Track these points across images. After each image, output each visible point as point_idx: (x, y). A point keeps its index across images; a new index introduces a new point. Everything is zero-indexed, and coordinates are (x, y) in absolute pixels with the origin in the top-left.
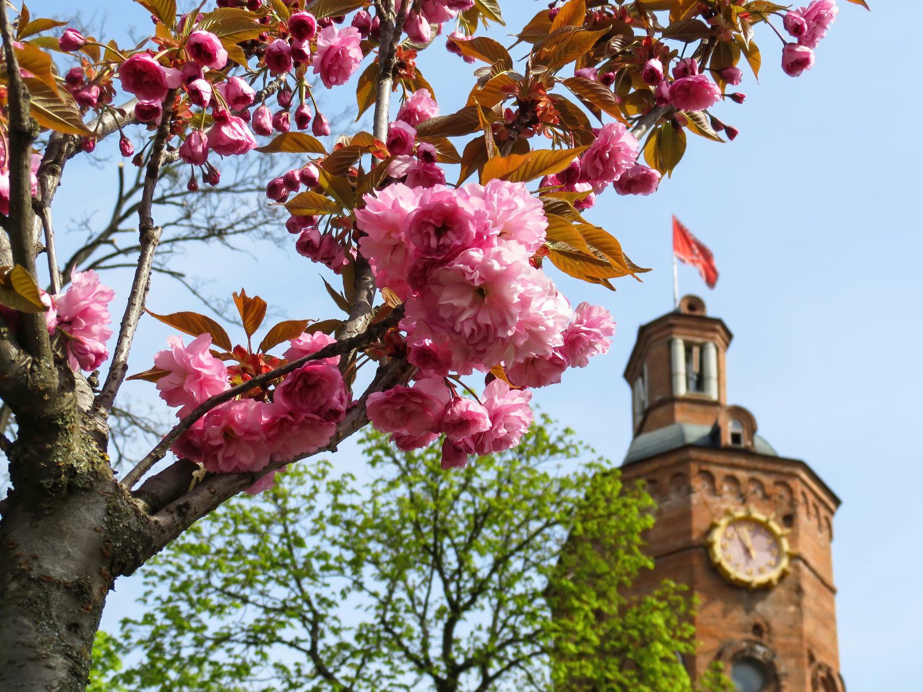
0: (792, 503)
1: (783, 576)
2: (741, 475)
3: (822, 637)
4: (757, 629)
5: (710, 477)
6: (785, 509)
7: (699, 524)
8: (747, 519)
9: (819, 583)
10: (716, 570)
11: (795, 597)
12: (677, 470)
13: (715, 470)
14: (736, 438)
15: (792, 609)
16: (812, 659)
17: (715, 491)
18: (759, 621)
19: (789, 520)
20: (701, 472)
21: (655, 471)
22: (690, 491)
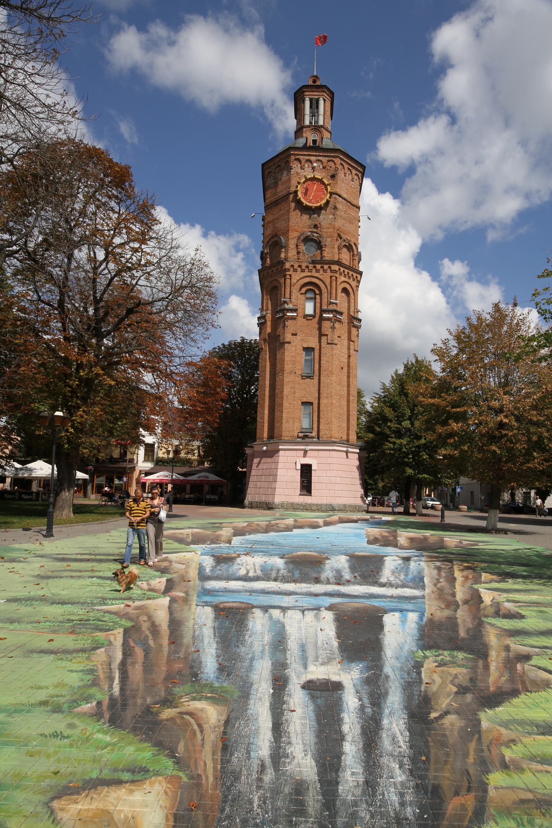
0: (336, 169)
1: (328, 202)
2: (313, 158)
3: (348, 227)
4: (316, 226)
5: (299, 160)
6: (332, 172)
7: (294, 182)
8: (313, 179)
9: (349, 204)
10: (299, 203)
11: (333, 211)
13: (301, 157)
14: (314, 141)
15: (331, 216)
16: (341, 238)
17: (302, 168)
18: (317, 223)
19: (333, 177)
20: (296, 159)
21: (279, 161)
22: (291, 168)
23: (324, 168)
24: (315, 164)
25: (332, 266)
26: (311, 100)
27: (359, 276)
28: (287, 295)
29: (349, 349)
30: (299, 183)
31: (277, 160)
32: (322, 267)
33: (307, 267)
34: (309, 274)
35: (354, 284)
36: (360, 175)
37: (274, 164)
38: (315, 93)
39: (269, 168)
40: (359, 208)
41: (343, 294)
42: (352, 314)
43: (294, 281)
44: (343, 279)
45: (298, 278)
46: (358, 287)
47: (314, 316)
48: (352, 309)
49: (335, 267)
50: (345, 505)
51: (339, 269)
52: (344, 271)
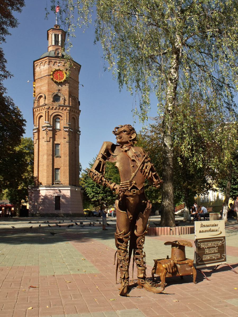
1: (65, 80)
12: (46, 61)
16: (71, 95)
18: (60, 89)
23: (63, 65)
24: (59, 65)
25: (67, 108)
26: (55, 35)
27: (79, 112)
28: (47, 120)
29: (75, 144)
30: (52, 71)
31: (41, 60)
32: (63, 108)
33: (56, 108)
34: (57, 111)
35: (77, 115)
36: (79, 68)
37: (40, 62)
38: (58, 32)
39: (37, 63)
40: (79, 83)
41: (72, 120)
42: (76, 128)
43: (50, 114)
44: (72, 113)
45: (52, 113)
46: (79, 117)
47: (60, 130)
48: (76, 127)
49: (68, 108)
50: (75, 214)
51: (71, 109)
52: (73, 110)
